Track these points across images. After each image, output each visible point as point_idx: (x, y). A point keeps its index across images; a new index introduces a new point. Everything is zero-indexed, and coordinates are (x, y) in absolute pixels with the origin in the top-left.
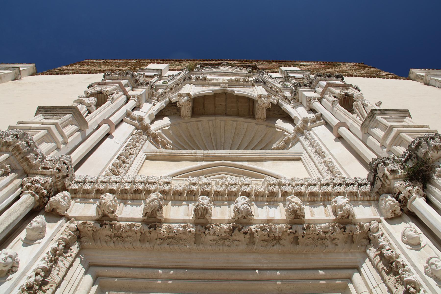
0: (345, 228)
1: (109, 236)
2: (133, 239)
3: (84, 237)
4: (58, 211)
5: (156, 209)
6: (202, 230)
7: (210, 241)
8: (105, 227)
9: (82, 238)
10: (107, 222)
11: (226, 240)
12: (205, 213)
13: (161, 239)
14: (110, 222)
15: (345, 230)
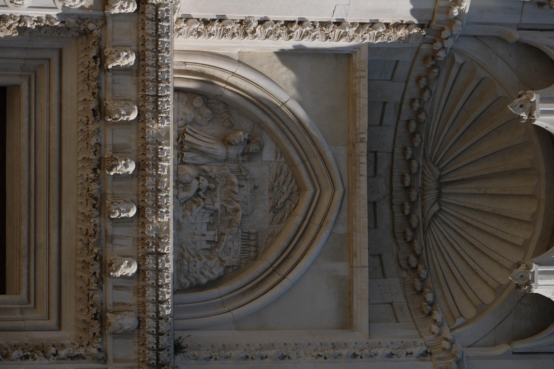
0: (95, 319)
1: (88, 66)
2: (87, 92)
3: (87, 38)
4: (106, 6)
5: (111, 115)
6: (93, 166)
7: (86, 174)
8: (93, 62)
9: (86, 36)
10: (99, 63)
11: (88, 191)
12: (108, 168)
13: (87, 122)
14: (97, 66)
15: (93, 320)
